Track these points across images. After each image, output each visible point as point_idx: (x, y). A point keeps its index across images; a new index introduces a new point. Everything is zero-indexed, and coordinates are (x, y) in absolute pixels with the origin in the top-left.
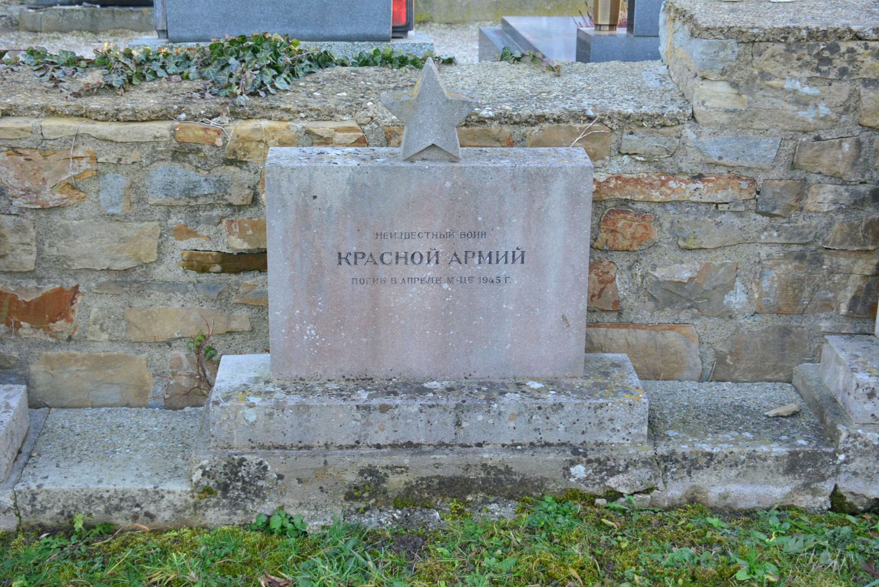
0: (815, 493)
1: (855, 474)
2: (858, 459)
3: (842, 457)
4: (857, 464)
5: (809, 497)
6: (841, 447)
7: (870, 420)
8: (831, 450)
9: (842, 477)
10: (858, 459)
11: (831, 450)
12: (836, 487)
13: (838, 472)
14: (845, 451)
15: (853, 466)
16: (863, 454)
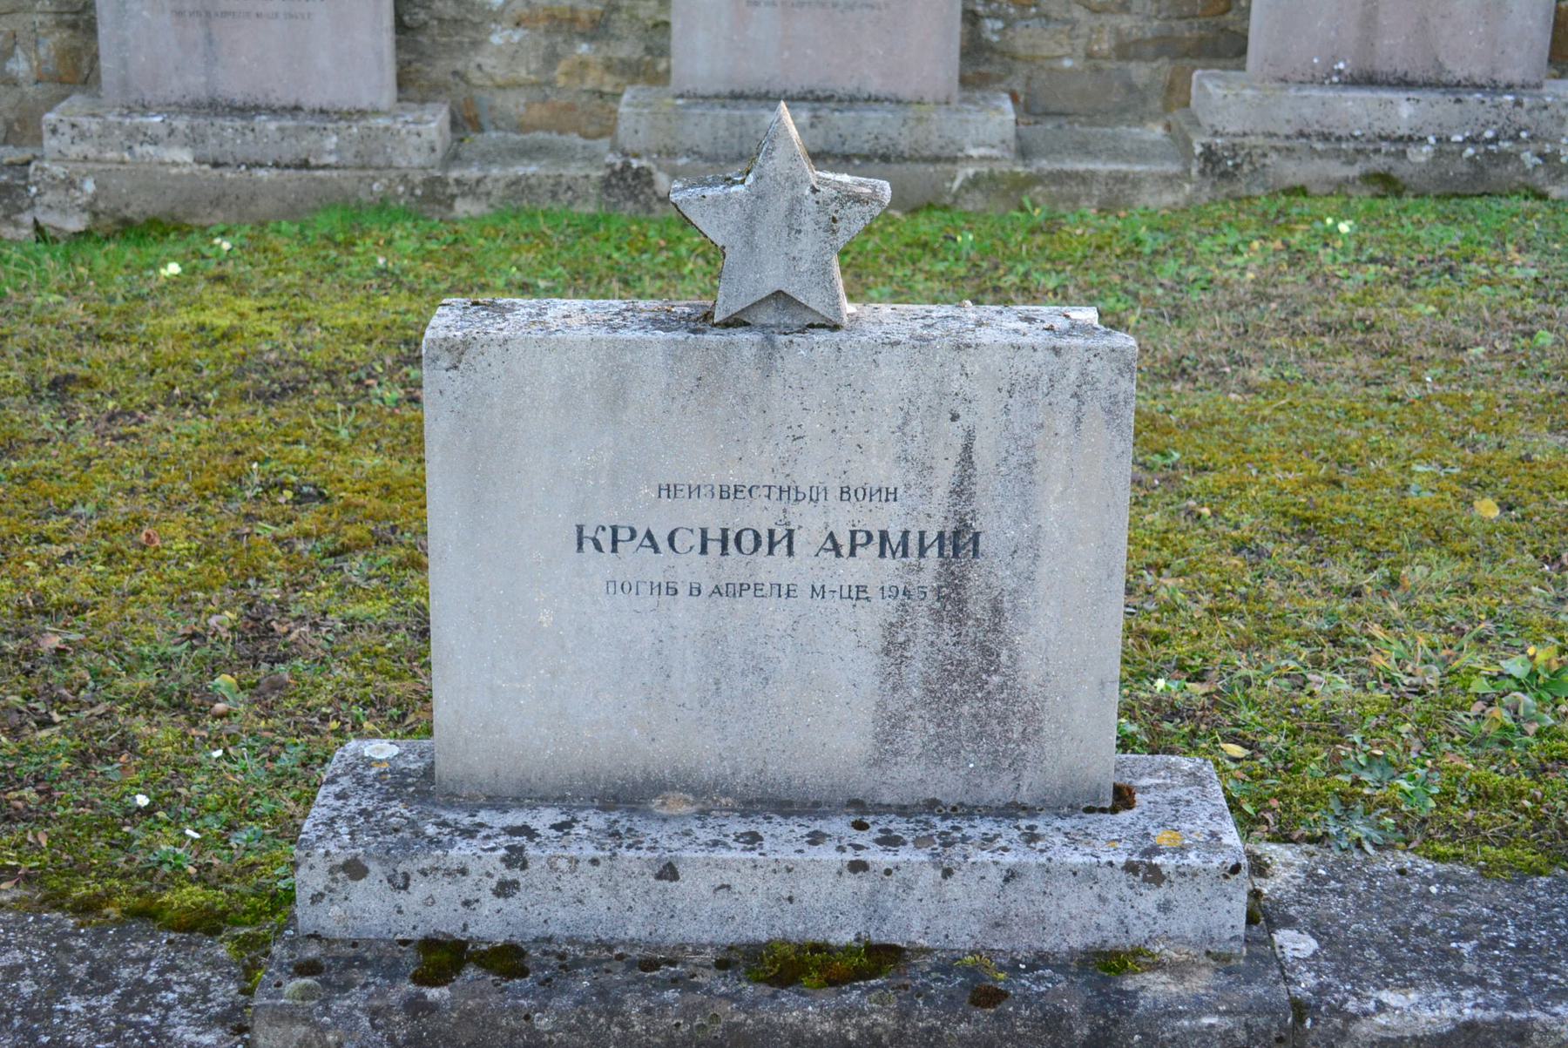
0: (17, 225)
1: (49, 207)
2: (49, 193)
3: (34, 190)
4: (49, 197)
5: (12, 229)
6: (31, 180)
7: (57, 156)
8: (22, 183)
9: (39, 210)
10: (49, 193)
11: (22, 183)
12: (36, 222)
13: (32, 205)
14: (36, 183)
15: (47, 198)
16: (53, 187)
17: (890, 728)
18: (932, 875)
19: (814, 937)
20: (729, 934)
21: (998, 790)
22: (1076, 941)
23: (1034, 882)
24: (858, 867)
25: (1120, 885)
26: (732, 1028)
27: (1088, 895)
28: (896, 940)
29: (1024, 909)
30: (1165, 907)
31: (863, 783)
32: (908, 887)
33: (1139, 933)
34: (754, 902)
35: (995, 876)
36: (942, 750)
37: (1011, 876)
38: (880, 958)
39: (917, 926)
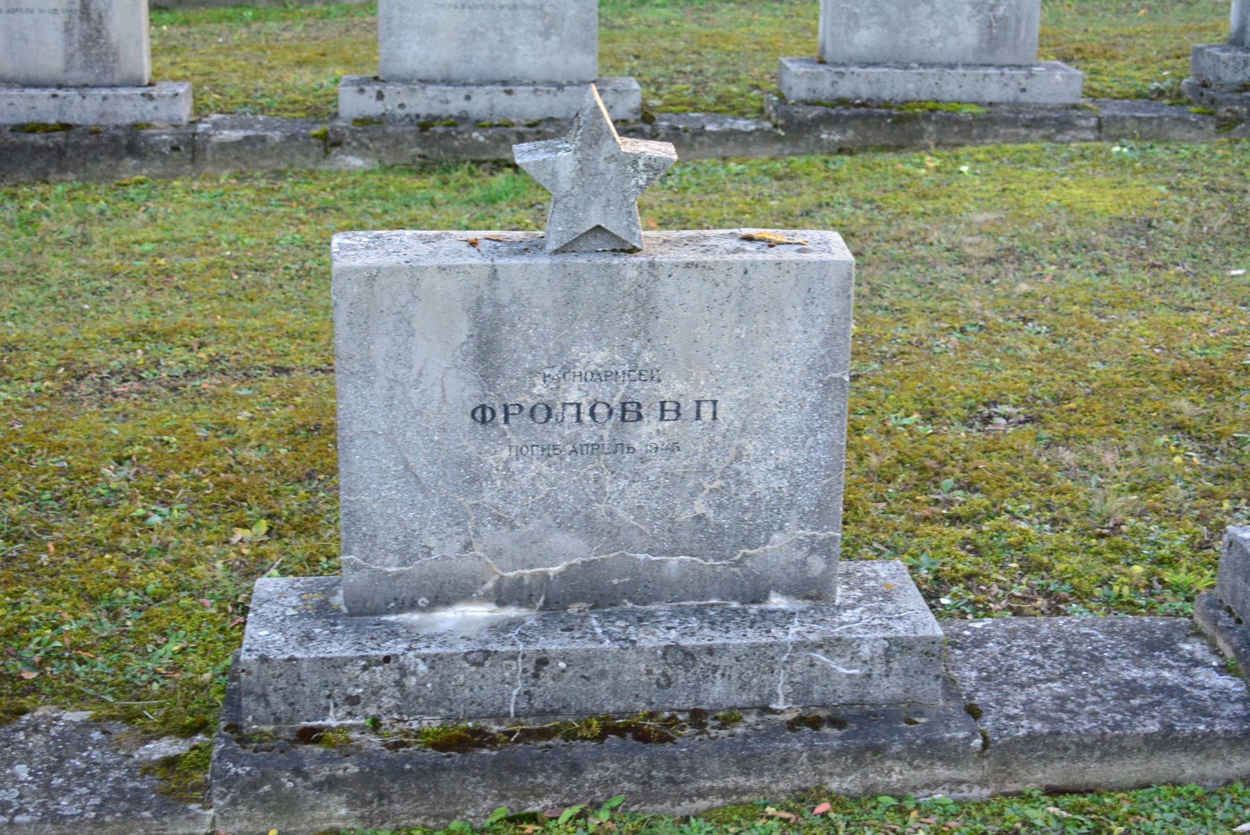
17: (69, 58)
18: (78, 98)
19: (42, 121)
20: (14, 121)
21: (107, 79)
22: (128, 121)
23: (112, 100)
24: (54, 96)
25: (140, 101)
26: (12, 143)
27: (130, 104)
28: (69, 121)
29: (109, 110)
30: (156, 108)
31: (62, 78)
32: (71, 102)
33: (148, 118)
34: (22, 109)
35: (99, 99)
36: (87, 66)
37: (105, 98)
38: (66, 127)
39: (76, 116)
